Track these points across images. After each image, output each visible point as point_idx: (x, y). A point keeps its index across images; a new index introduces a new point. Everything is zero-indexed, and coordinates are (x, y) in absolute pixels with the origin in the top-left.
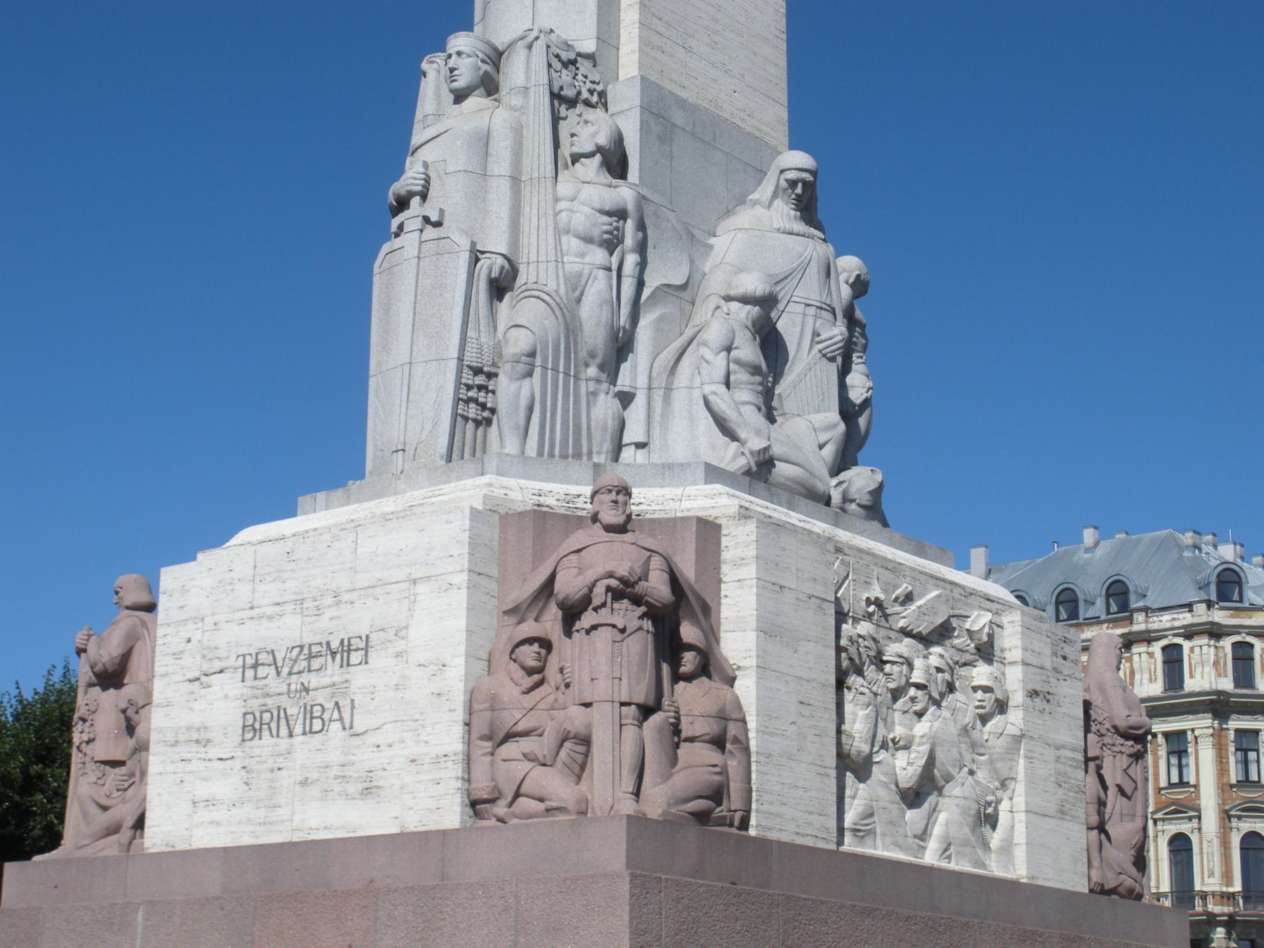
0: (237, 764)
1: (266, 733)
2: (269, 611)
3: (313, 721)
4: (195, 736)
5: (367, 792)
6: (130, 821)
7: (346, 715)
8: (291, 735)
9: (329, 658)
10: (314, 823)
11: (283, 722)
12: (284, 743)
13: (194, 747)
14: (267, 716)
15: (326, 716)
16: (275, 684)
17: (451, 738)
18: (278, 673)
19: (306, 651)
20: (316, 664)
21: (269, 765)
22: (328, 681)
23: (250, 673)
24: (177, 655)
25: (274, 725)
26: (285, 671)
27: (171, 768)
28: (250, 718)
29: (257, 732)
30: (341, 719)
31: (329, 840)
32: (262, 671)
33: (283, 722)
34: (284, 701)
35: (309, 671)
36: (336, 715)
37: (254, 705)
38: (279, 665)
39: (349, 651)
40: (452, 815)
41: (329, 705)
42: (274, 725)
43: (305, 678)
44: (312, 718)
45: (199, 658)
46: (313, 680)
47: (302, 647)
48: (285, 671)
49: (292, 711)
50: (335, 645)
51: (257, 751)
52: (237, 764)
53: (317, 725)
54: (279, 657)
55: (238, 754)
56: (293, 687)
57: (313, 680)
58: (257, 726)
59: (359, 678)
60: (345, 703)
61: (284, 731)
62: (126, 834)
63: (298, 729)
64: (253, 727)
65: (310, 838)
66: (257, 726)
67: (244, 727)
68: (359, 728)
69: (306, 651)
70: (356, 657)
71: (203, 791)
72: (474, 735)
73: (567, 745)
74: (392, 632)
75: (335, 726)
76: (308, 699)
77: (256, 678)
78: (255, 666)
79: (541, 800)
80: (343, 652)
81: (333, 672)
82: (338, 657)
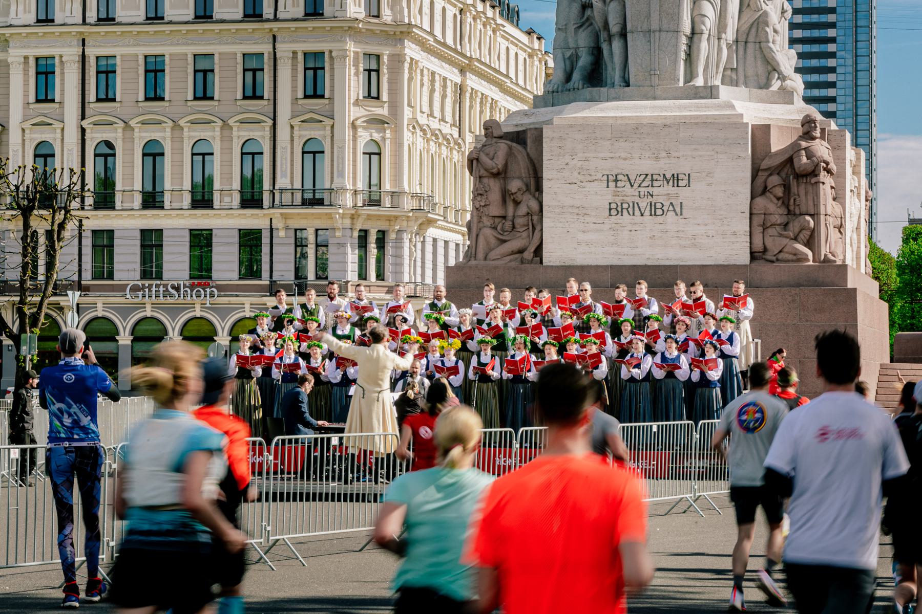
0: (607, 226)
1: (625, 212)
2: (623, 155)
3: (654, 210)
4: (576, 211)
5: (694, 245)
6: (532, 249)
7: (678, 210)
8: (642, 215)
9: (665, 182)
10: (659, 256)
11: (636, 208)
12: (638, 218)
13: (575, 217)
14: (625, 206)
15: (665, 208)
16: (628, 189)
17: (744, 226)
18: (632, 186)
19: (649, 177)
20: (655, 183)
21: (629, 227)
22: (665, 193)
23: (612, 184)
24: (560, 170)
25: (631, 210)
26: (636, 185)
27: (561, 225)
28: (614, 206)
29: (620, 212)
30: (674, 210)
31: (677, 266)
32: (619, 184)
33: (636, 208)
34: (637, 199)
35: (652, 186)
36: (671, 208)
37: (618, 200)
38: (632, 182)
39: (678, 180)
40: (744, 258)
41: (667, 204)
42: (631, 210)
43: (650, 189)
44: (655, 209)
45: (576, 174)
46: (655, 191)
47: (647, 175)
48: (636, 185)
49: (643, 204)
50: (668, 176)
51: (620, 221)
52: (607, 226)
53: (659, 212)
54: (632, 178)
55: (607, 221)
56: (642, 193)
57: (655, 191)
58: (619, 209)
59: (683, 193)
60: (677, 204)
61: (637, 212)
62: (528, 255)
63: (647, 213)
64: (616, 209)
65: (657, 264)
66: (619, 209)
67: (610, 209)
68: (685, 215)
69: (649, 177)
70: (680, 183)
71: (581, 236)
72: (755, 223)
73: (804, 232)
74: (704, 174)
75: (671, 214)
76: (654, 200)
77: (616, 187)
78: (616, 181)
79: (795, 255)
80: (676, 179)
81: (669, 189)
82: (671, 182)
